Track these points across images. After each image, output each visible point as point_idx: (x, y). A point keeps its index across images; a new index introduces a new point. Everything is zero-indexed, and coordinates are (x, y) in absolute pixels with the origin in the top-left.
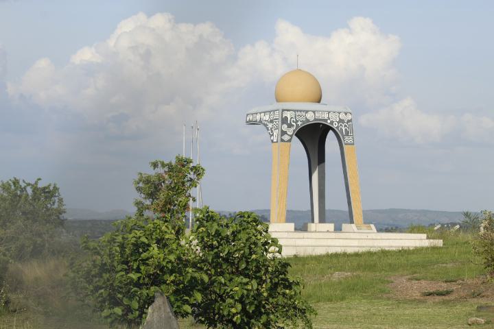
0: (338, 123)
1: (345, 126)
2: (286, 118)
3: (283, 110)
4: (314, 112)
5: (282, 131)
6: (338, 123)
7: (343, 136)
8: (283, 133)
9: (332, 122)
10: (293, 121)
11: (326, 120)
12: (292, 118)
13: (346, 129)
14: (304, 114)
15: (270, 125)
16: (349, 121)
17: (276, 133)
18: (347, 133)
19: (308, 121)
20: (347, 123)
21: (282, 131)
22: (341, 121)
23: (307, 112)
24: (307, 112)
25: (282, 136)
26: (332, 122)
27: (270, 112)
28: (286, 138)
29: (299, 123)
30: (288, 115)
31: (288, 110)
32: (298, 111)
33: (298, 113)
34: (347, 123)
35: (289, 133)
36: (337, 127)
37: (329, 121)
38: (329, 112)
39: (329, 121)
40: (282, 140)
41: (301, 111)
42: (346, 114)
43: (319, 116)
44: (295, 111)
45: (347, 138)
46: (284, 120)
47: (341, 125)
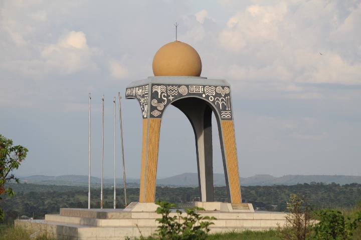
0: (214, 97)
1: (222, 100)
2: (156, 93)
3: (153, 85)
4: (187, 86)
5: (151, 106)
6: (214, 97)
7: (220, 111)
8: (153, 108)
9: (207, 97)
10: (164, 96)
11: (201, 95)
12: (162, 93)
13: (223, 104)
14: (176, 88)
15: (142, 100)
16: (226, 95)
17: (146, 108)
18: (224, 108)
19: (180, 95)
20: (225, 97)
21: (151, 106)
22: (218, 95)
23: (179, 86)
24: (179, 86)
25: (151, 111)
26: (207, 97)
27: (142, 86)
28: (156, 113)
29: (171, 98)
30: (159, 90)
31: (158, 85)
32: (169, 85)
33: (169, 88)
34: (225, 97)
35: (159, 108)
36: (214, 102)
37: (204, 96)
38: (204, 86)
39: (204, 96)
40: (152, 116)
41: (172, 85)
42: (223, 87)
43: (194, 90)
44: (166, 85)
45: (224, 112)
46: (154, 95)
47: (218, 99)
